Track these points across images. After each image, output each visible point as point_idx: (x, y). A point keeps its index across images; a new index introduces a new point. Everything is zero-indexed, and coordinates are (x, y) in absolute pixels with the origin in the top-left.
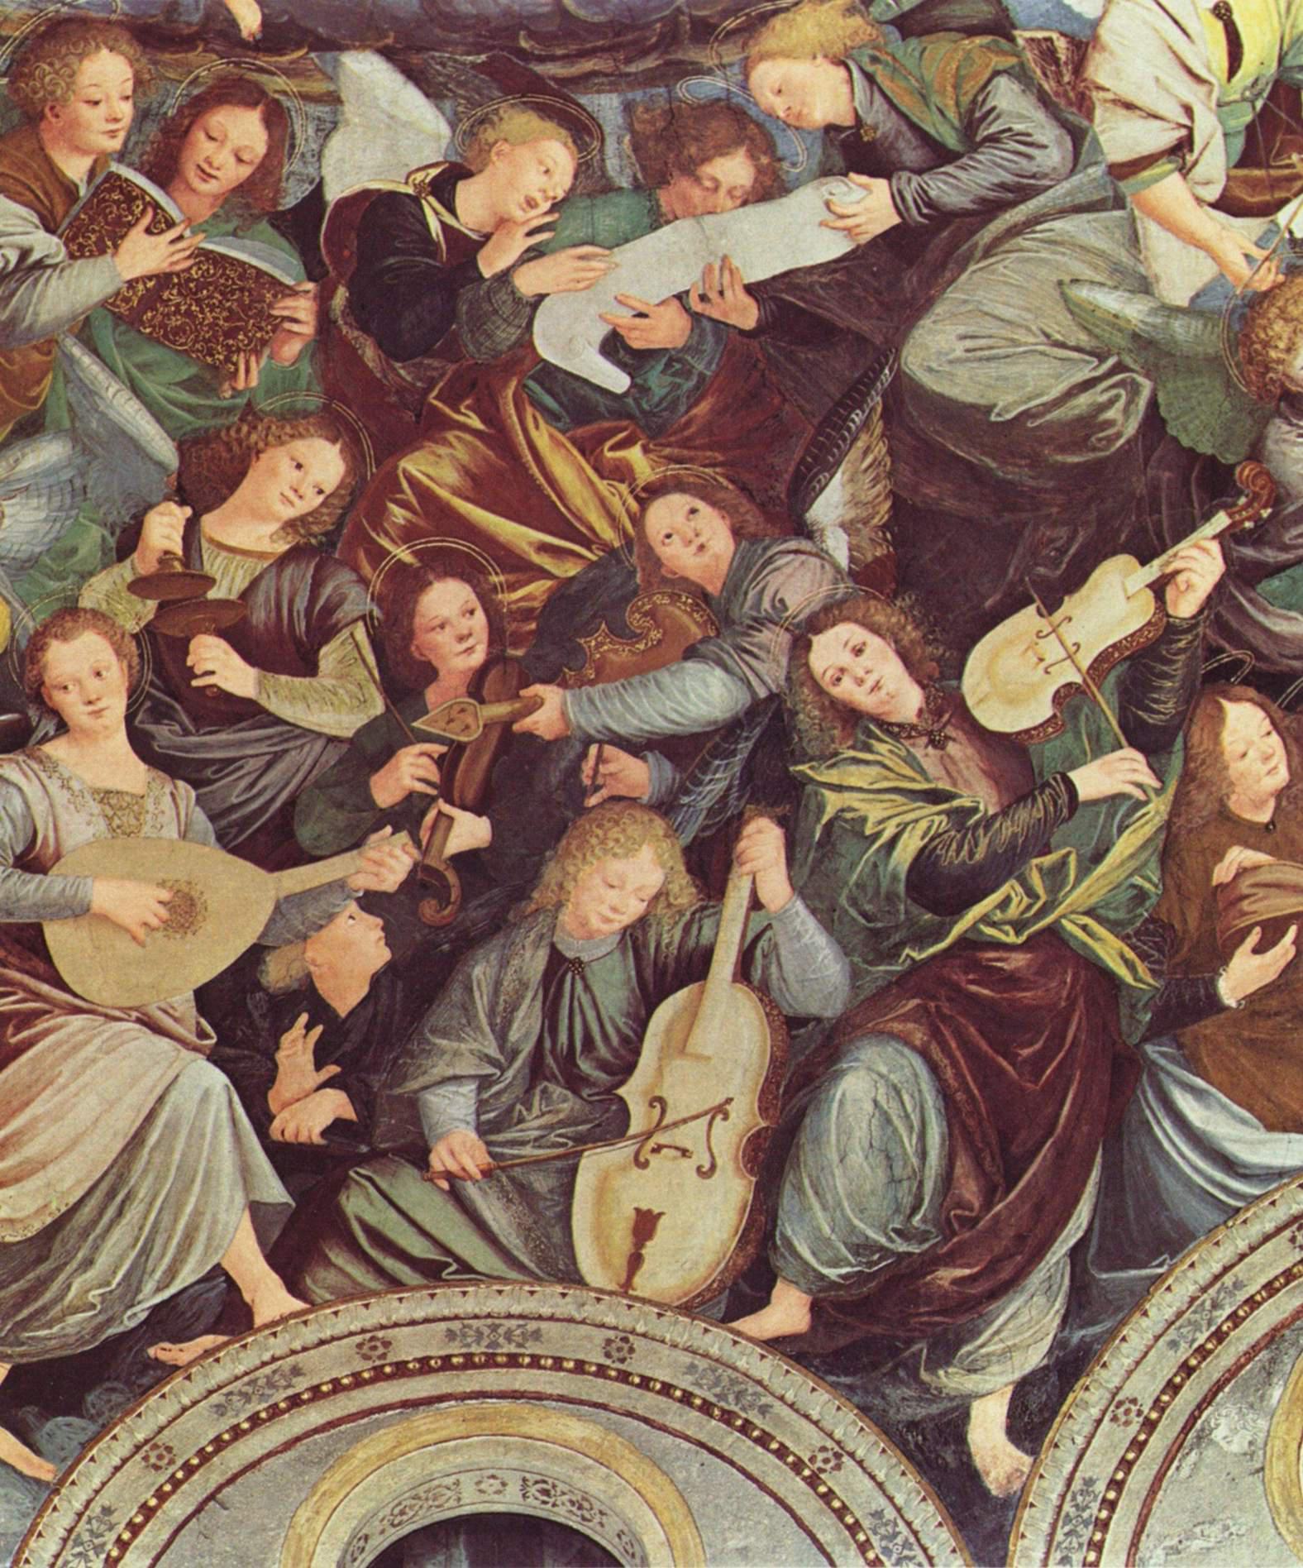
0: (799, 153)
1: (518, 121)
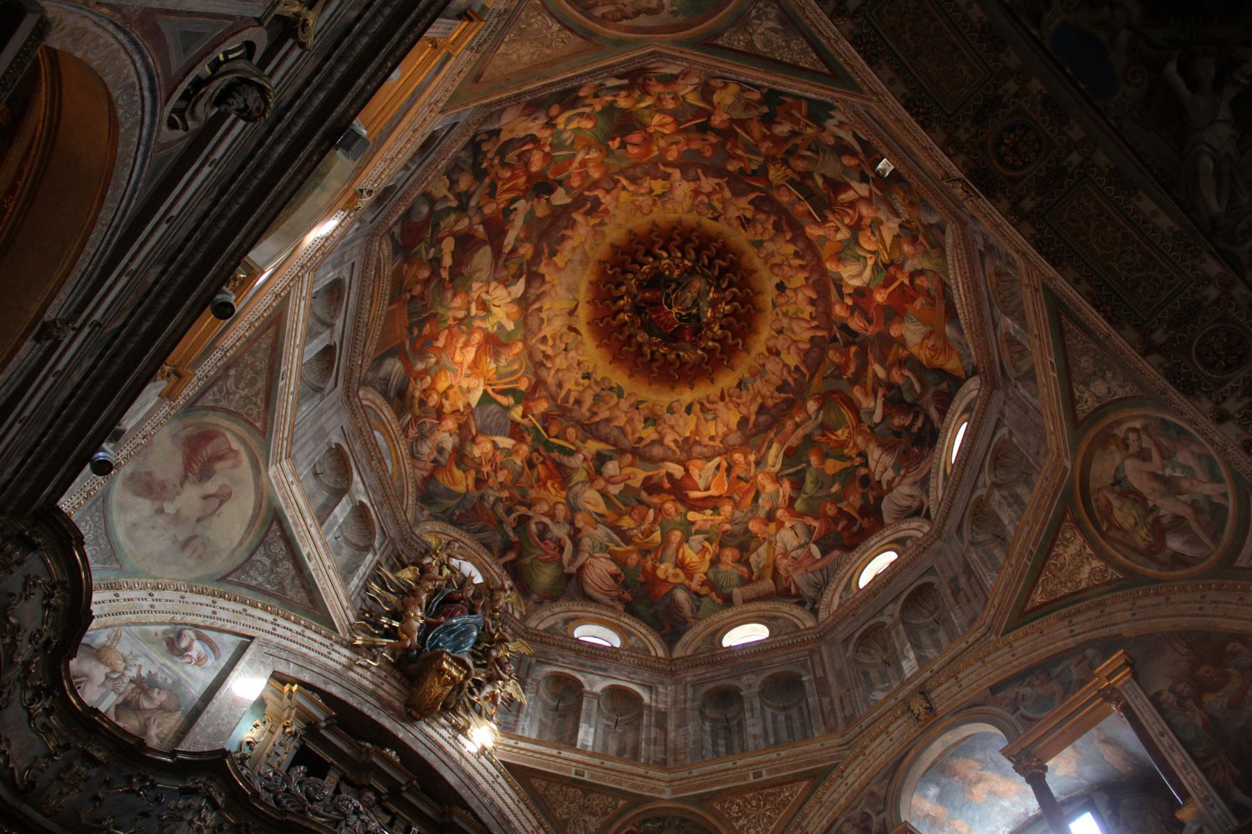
1: (547, 212)
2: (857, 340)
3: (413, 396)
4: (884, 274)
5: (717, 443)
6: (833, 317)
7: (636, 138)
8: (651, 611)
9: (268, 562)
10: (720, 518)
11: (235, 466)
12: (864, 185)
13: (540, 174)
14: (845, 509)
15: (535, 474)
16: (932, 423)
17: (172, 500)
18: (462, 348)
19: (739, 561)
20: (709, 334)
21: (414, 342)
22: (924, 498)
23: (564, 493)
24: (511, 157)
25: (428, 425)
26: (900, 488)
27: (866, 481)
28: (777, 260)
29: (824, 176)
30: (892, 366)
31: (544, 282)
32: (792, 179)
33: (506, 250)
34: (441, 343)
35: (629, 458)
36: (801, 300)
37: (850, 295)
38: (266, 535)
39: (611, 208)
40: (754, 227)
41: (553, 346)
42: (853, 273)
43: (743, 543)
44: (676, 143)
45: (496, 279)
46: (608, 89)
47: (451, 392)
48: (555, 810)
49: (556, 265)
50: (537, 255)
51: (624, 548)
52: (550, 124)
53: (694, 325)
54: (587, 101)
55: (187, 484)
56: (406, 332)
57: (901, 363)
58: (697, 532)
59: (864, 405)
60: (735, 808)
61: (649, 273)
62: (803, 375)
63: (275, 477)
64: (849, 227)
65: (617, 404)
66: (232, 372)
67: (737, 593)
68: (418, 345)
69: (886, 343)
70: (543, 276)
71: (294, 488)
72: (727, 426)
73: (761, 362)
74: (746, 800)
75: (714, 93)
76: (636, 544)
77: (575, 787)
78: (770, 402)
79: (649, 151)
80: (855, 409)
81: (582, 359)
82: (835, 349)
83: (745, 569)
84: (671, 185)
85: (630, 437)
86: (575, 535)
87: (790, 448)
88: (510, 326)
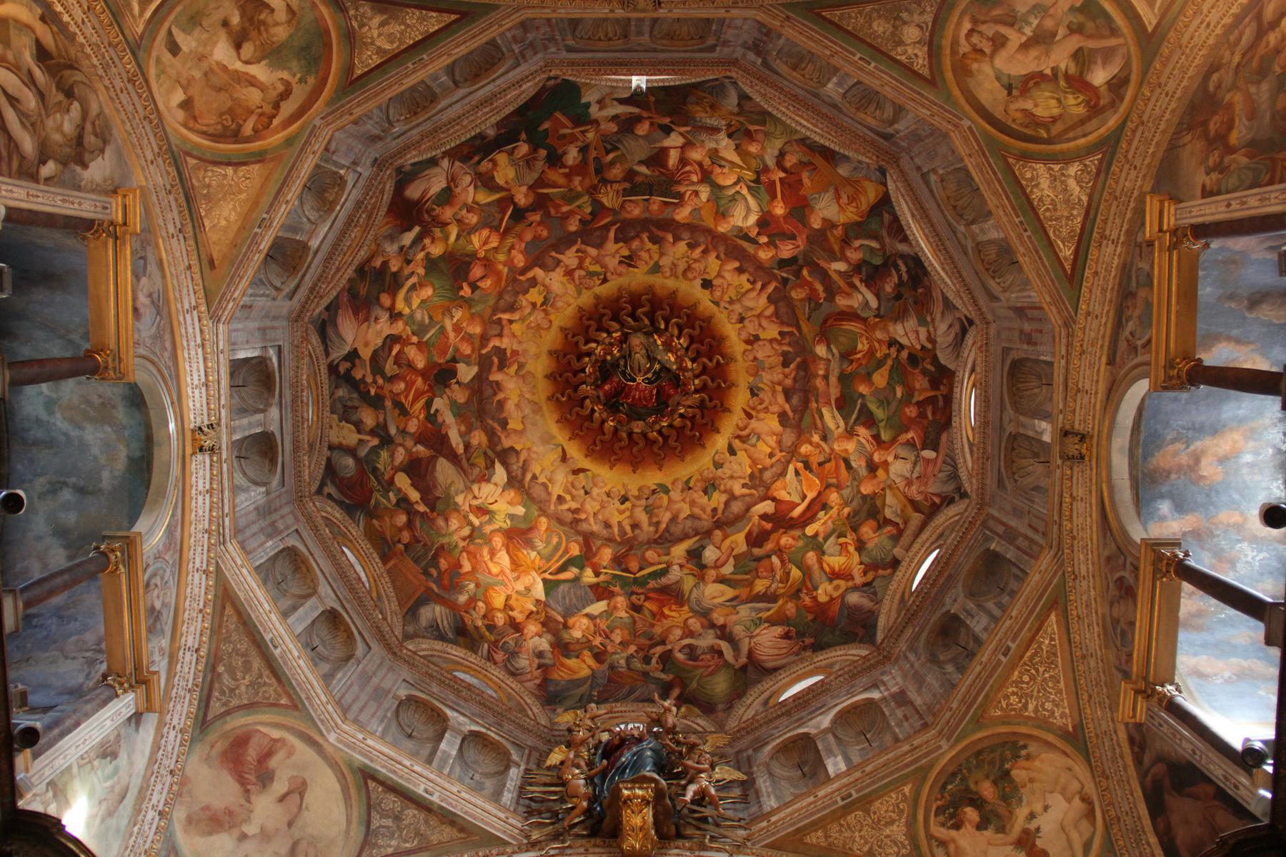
0: (467, 438)
1: (467, 393)
2: (801, 262)
3: (477, 628)
4: (763, 189)
5: (779, 455)
6: (767, 265)
7: (477, 272)
8: (837, 633)
9: (389, 822)
10: (834, 512)
11: (291, 753)
12: (673, 135)
13: (431, 366)
14: (921, 398)
15: (646, 612)
16: (909, 255)
17: (248, 820)
18: (491, 559)
19: (879, 527)
20: (688, 374)
21: (438, 582)
22: (958, 315)
23: (686, 608)
24: (390, 368)
25: (512, 643)
26: (940, 332)
27: (913, 359)
28: (682, 266)
29: (641, 162)
30: (842, 252)
31: (517, 453)
32: (624, 190)
33: (460, 450)
34: (467, 566)
35: (718, 534)
36: (732, 279)
37: (759, 234)
38: (369, 798)
39: (515, 347)
40: (639, 258)
41: (573, 498)
42: (743, 214)
43: (870, 510)
44: (512, 247)
45: (473, 482)
46: (411, 247)
47: (512, 602)
48: (851, 849)
49: (515, 431)
50: (492, 435)
51: (775, 607)
52: (395, 316)
53: (668, 380)
54: (406, 272)
55: (253, 798)
56: (423, 577)
57: (846, 241)
58: (826, 539)
59: (856, 306)
61: (595, 371)
62: (791, 334)
63: (340, 742)
64: (701, 181)
65: (670, 500)
66: (221, 669)
67: (897, 551)
68: (446, 582)
69: (819, 238)
70: (512, 448)
71: (369, 742)
72: (774, 434)
73: (751, 357)
75: (493, 177)
76: (782, 595)
77: (851, 812)
78: (788, 382)
79: (499, 274)
80: (851, 315)
81: (607, 489)
82: (793, 288)
83: (889, 528)
84: (544, 285)
85: (704, 516)
86: (724, 633)
87: (837, 400)
88: (520, 510)
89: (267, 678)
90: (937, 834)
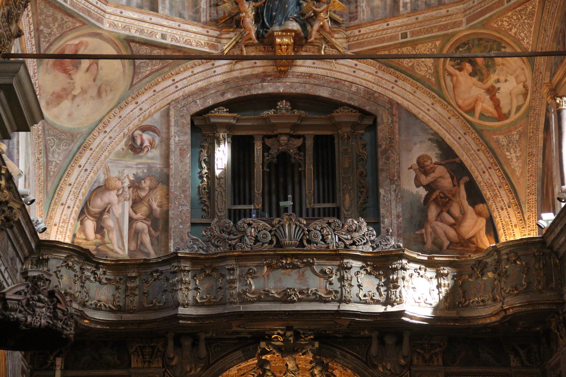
11: (87, 46)
55: (73, 77)
60: (505, 24)
66: (41, 28)
74: (509, 18)
89: (66, 18)
90: (449, 70)
